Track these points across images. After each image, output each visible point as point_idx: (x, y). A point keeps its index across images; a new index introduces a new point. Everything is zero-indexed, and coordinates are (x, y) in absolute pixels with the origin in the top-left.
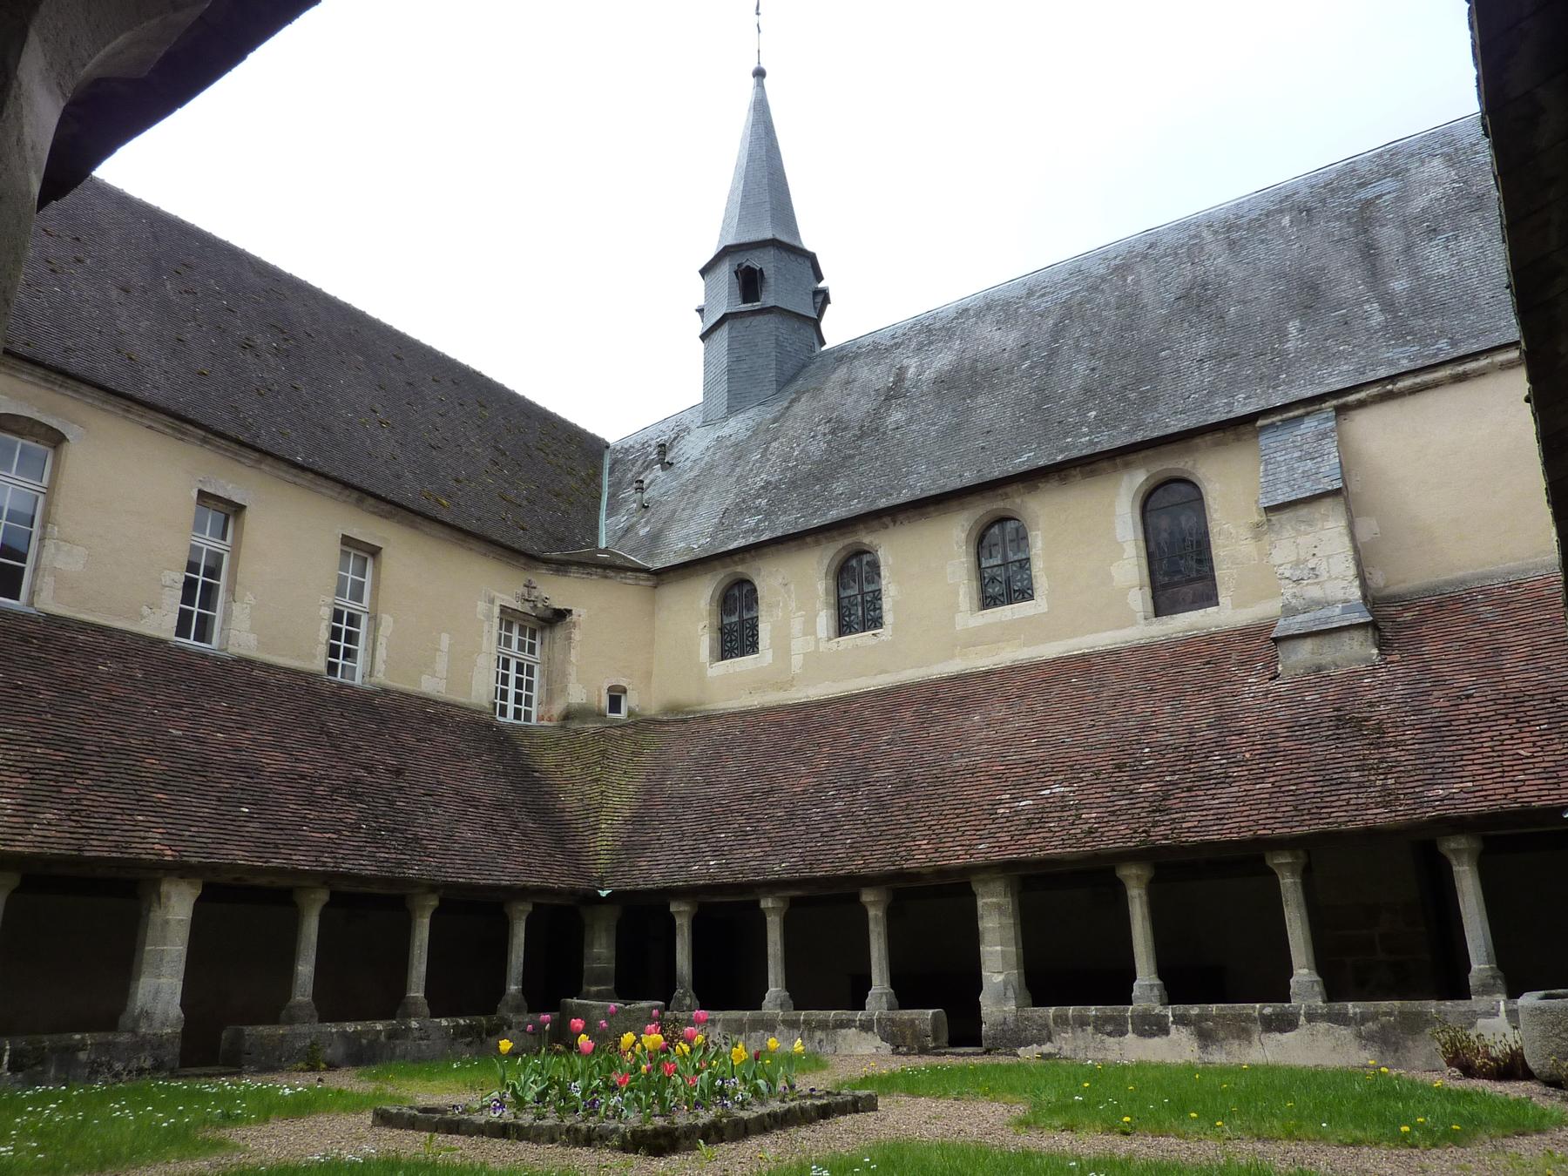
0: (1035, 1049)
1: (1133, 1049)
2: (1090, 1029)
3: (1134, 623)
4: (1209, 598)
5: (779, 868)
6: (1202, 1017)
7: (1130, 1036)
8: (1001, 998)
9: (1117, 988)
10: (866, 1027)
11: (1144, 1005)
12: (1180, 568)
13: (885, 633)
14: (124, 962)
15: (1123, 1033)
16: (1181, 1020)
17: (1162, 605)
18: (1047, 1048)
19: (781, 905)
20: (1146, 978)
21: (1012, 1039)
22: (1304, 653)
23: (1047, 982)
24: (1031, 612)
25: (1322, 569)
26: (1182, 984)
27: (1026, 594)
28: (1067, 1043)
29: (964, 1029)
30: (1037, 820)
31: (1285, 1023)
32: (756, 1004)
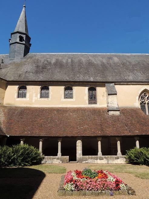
0: (85, 162)
1: (99, 161)
2: (93, 159)
3: (86, 104)
4: (95, 103)
5: (43, 134)
6: (108, 157)
7: (98, 160)
8: (80, 155)
9: (96, 153)
10: (58, 159)
11: (100, 156)
12: (93, 98)
13: (49, 99)
14: (135, 145)
15: (97, 160)
16: (105, 158)
17: (90, 103)
18: (87, 162)
19: (119, 139)
20: (100, 152)
21: (81, 161)
22: (111, 113)
23: (85, 152)
24: (73, 100)
25: (114, 103)
26: (104, 153)
27: (72, 97)
28: (89, 161)
29: (73, 158)
30: (85, 130)
31: (118, 158)
32: (57, 155)
